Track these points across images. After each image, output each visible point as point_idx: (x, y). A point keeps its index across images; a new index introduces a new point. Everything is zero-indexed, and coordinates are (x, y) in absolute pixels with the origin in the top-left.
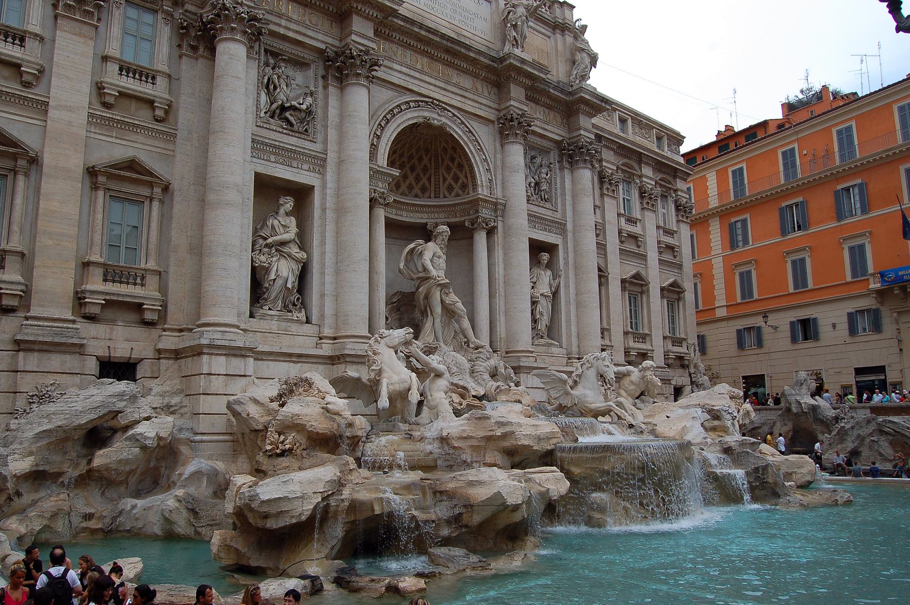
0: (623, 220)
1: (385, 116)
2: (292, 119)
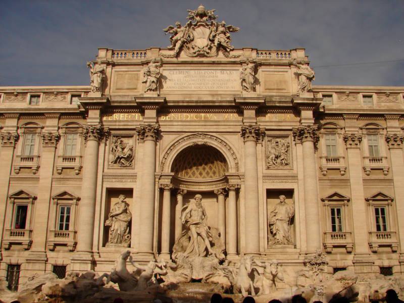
0: (367, 161)
1: (170, 148)
2: (123, 162)
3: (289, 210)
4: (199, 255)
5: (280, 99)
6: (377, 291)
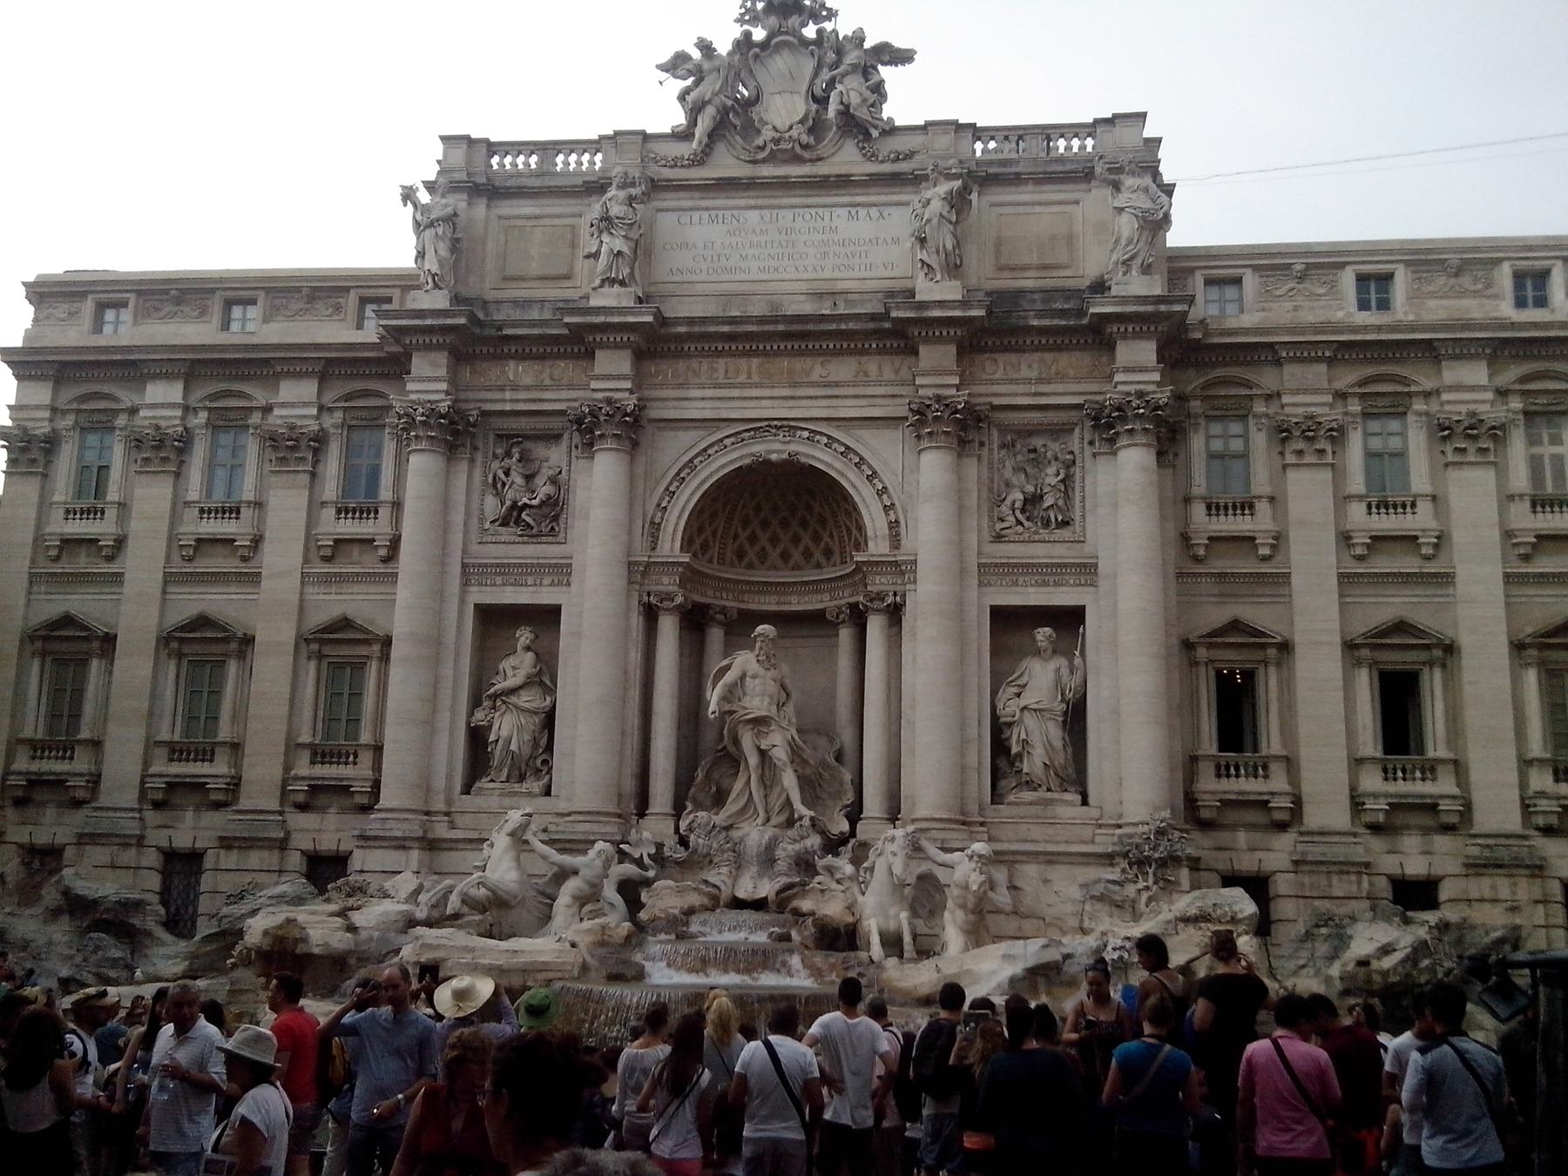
1: (678, 474)
2: (529, 520)
3: (1065, 679)
4: (768, 820)
5: (1044, 301)
6: (1363, 963)
